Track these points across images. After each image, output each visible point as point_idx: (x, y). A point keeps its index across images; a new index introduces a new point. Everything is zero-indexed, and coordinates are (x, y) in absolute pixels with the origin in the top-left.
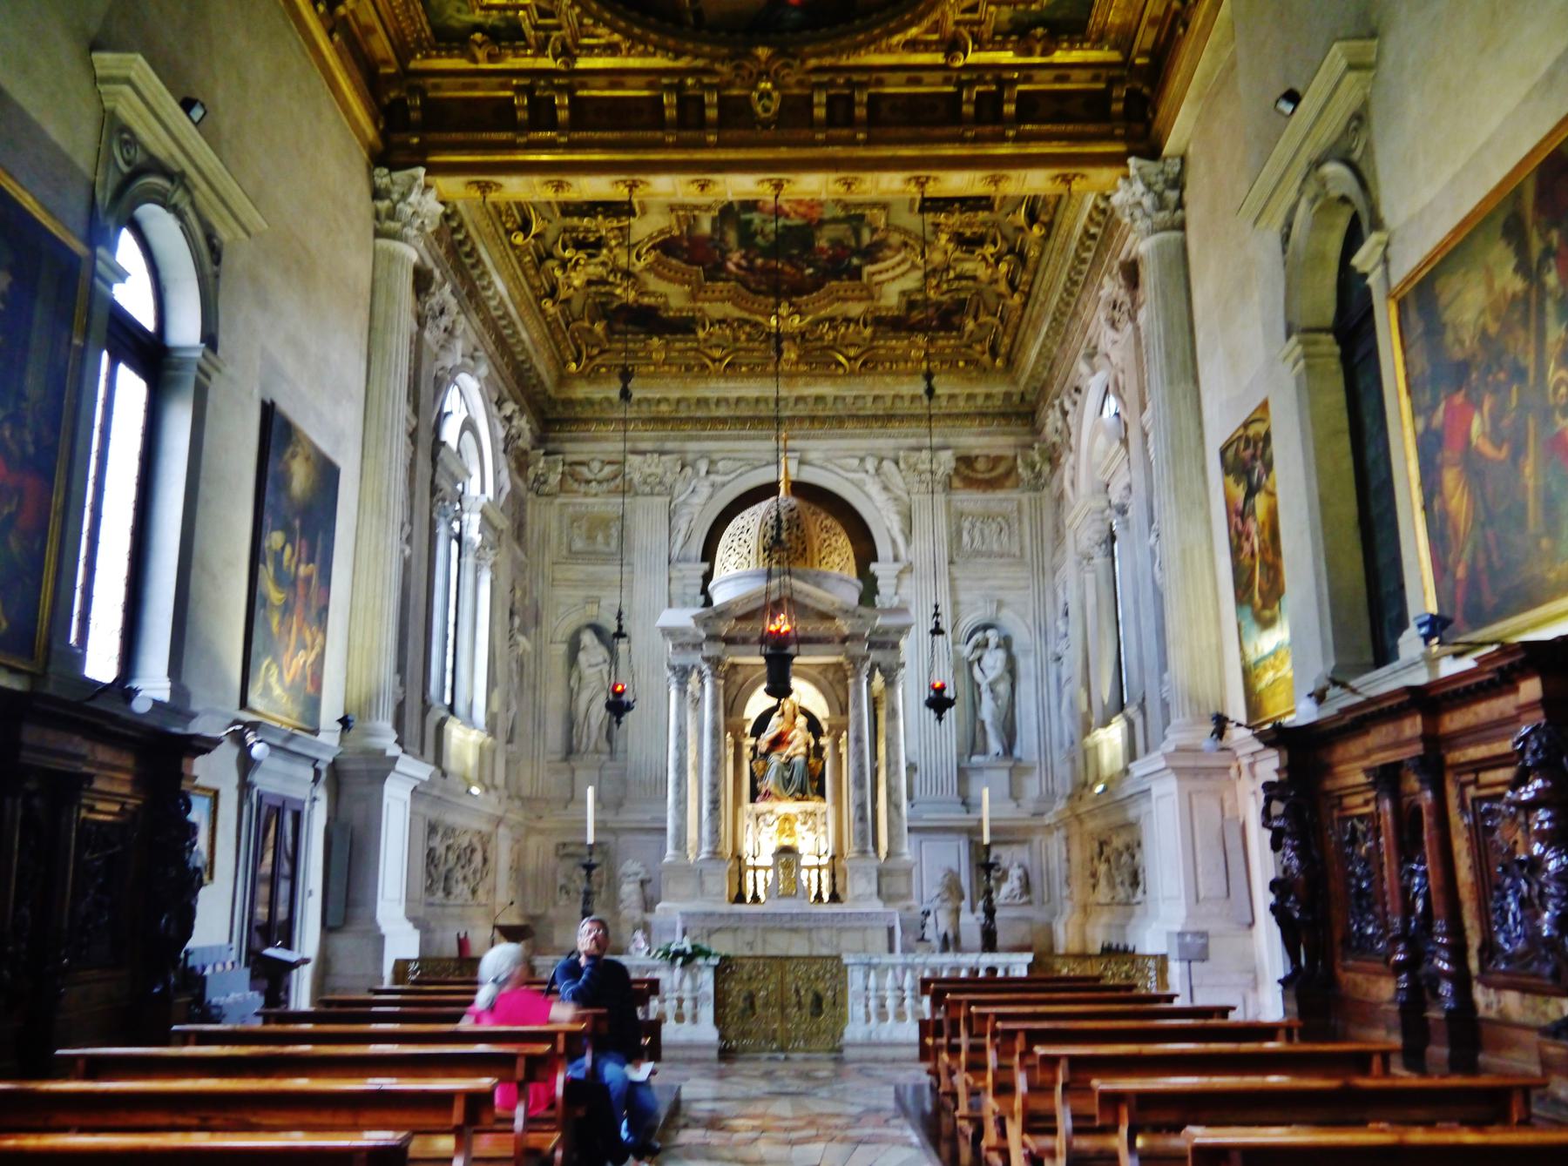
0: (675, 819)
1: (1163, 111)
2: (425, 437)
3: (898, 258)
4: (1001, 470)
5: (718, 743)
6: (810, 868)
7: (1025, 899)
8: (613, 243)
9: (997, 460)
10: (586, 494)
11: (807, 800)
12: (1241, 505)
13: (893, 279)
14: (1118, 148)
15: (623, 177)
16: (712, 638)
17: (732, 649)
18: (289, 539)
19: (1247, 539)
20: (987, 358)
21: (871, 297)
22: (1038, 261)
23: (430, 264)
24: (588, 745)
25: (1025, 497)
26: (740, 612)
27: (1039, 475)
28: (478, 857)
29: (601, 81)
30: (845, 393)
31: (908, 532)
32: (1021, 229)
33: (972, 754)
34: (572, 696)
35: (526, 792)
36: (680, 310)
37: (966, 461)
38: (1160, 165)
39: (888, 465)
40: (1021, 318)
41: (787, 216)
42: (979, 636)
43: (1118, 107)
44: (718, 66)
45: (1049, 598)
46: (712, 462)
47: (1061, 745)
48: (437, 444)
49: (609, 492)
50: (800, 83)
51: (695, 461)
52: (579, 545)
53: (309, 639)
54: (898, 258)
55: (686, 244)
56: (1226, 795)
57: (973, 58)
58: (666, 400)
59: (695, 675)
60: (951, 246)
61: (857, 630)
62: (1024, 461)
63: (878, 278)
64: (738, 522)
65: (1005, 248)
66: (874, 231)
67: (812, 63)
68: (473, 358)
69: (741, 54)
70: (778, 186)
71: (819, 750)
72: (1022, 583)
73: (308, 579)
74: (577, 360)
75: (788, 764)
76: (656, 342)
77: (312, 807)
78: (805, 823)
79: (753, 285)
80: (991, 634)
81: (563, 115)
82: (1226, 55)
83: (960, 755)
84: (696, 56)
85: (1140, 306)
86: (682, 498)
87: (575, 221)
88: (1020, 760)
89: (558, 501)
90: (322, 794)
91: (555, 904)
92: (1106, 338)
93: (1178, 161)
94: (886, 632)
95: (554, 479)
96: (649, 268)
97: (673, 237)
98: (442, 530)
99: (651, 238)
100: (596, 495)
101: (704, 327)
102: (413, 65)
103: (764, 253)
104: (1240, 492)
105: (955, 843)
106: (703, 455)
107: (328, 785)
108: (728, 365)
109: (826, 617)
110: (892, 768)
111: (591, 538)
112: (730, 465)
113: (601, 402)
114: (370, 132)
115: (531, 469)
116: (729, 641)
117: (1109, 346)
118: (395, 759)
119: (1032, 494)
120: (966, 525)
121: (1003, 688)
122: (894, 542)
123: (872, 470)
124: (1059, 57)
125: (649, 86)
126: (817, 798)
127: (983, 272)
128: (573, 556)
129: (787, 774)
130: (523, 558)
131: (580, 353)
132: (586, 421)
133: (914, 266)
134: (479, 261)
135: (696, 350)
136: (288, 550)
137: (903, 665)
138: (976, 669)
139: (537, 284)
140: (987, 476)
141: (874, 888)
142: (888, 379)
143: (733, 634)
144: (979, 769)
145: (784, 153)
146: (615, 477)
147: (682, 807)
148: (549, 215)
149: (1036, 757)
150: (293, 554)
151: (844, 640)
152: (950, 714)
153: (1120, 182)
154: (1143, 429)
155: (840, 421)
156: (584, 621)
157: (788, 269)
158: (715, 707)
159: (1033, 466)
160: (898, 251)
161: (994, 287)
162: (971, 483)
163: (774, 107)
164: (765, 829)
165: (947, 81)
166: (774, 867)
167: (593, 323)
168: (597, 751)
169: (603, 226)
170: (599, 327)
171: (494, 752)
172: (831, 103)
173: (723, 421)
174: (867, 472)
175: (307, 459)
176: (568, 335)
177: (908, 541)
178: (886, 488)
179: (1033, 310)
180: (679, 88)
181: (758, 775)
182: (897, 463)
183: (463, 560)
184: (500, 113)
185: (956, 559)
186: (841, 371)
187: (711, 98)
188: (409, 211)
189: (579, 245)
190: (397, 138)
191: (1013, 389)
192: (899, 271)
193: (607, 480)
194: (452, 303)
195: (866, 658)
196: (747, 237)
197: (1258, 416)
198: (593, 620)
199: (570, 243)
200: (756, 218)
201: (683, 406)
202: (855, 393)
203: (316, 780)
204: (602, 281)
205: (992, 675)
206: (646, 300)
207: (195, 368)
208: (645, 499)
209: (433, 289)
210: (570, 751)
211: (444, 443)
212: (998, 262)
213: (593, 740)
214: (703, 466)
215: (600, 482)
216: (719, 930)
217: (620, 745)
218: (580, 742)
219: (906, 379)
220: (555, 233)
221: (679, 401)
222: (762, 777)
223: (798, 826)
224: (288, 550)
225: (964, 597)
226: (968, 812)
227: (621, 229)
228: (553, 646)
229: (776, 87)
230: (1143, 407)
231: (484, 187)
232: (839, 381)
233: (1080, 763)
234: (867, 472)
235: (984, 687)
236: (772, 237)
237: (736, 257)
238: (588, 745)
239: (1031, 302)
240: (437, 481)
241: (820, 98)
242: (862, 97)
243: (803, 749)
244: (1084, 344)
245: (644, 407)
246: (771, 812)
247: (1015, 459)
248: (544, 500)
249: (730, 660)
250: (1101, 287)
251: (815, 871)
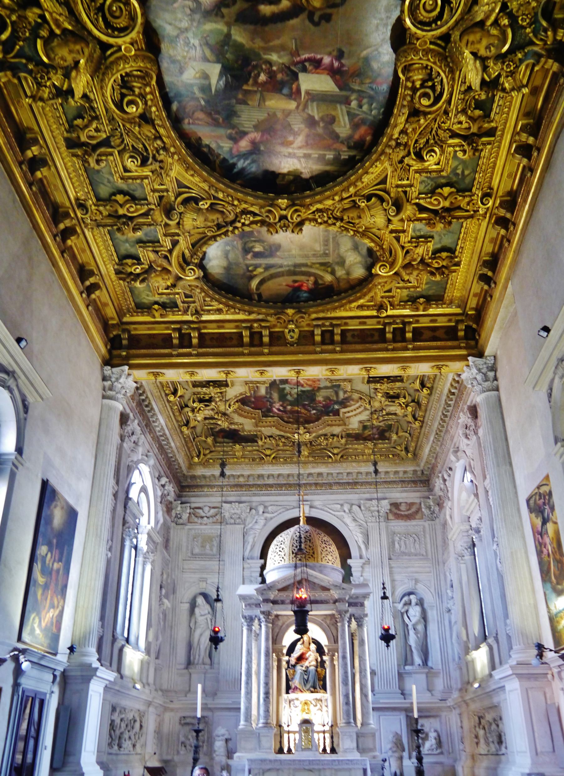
1: (483, 335)
2: (121, 496)
3: (358, 405)
4: (413, 509)
5: (269, 659)
6: (318, 732)
7: (439, 751)
8: (218, 399)
9: (411, 505)
10: (201, 524)
12: (540, 529)
13: (355, 415)
14: (464, 352)
15: (223, 369)
16: (266, 601)
17: (276, 606)
18: (50, 550)
19: (545, 547)
20: (403, 453)
21: (345, 424)
22: (427, 406)
23: (128, 411)
24: (199, 660)
25: (426, 524)
26: (280, 586)
27: (433, 512)
28: (137, 725)
29: (214, 325)
30: (332, 472)
31: (367, 543)
32: (418, 390)
33: (406, 665)
34: (191, 631)
35: (165, 687)
36: (250, 431)
37: (395, 505)
38: (484, 360)
39: (355, 508)
40: (420, 433)
41: (302, 386)
42: (406, 598)
43: (461, 334)
44: (269, 318)
45: (442, 578)
46: (265, 507)
47: (454, 660)
48: (127, 499)
49: (214, 523)
50: (308, 325)
51: (257, 506)
52: (197, 550)
53: (56, 603)
54: (358, 405)
55: (253, 400)
56: (547, 690)
57: (390, 312)
58: (243, 476)
59: (256, 621)
60: (383, 399)
61: (341, 597)
62: (425, 505)
63: (347, 415)
64: (279, 539)
65: (410, 400)
66: (345, 392)
67: (314, 316)
68: (147, 456)
69: (280, 312)
70: (298, 372)
71: (323, 662)
72: (428, 570)
73: (58, 571)
74: (198, 456)
75: (306, 671)
76: (237, 447)
77: (51, 696)
79: (286, 419)
80: (412, 597)
81: (195, 341)
82: (512, 310)
83: (399, 665)
84: (259, 314)
85: (479, 427)
86: (250, 525)
87: (199, 389)
88: (432, 668)
89: (187, 527)
90: (56, 689)
91: (178, 753)
92: (463, 443)
93: (493, 358)
94: (357, 597)
95: (185, 516)
96: (235, 411)
97: (247, 396)
98: (127, 543)
99: (236, 397)
100: (206, 524)
101: (261, 439)
102: (125, 319)
103: (292, 404)
104: (539, 522)
105: (398, 717)
106: (261, 503)
107: (60, 684)
108: (274, 458)
109: (325, 589)
110: (363, 673)
111: (203, 546)
112: (274, 508)
113: (210, 477)
114: (103, 350)
115: (173, 511)
116: (274, 602)
117: (465, 447)
118: (96, 669)
119: (430, 522)
120: (397, 539)
121: (420, 627)
122: (359, 547)
123: (347, 511)
124: (431, 311)
125: (237, 327)
127: (399, 411)
128: (194, 556)
129: (306, 677)
130: (168, 557)
131: (200, 453)
132: (202, 486)
133: (366, 409)
134: (152, 409)
135: (258, 451)
136: (49, 555)
137: (366, 615)
138: (405, 617)
139: (180, 419)
140: (406, 513)
141: (355, 745)
142: (354, 464)
143: (276, 599)
144: (409, 673)
145: (301, 357)
146: (216, 515)
147: (249, 696)
148: (186, 387)
149: (440, 667)
150: (51, 557)
151: (335, 602)
152: (393, 643)
153: (465, 368)
154: (485, 488)
155: (330, 485)
156: (199, 591)
157: (303, 411)
158: (267, 639)
159: (429, 508)
160: (358, 402)
161: (406, 418)
162: (398, 516)
163: (296, 336)
165: (379, 323)
166: (300, 732)
167: (206, 437)
168: (204, 664)
169: (212, 391)
170: (210, 440)
171: (148, 664)
172: (323, 333)
173: (271, 486)
174: (345, 511)
175: (62, 508)
176: (194, 444)
177: (367, 548)
178: (355, 520)
179: (425, 430)
180: (250, 328)
181: (290, 677)
182: (360, 507)
183: (137, 559)
184: (166, 341)
185: (392, 557)
186: (330, 460)
187: (266, 332)
188: (120, 386)
189: (201, 401)
190: (115, 352)
191: (417, 469)
192: (358, 411)
193: (212, 517)
194: (138, 430)
195: (346, 612)
196: (283, 397)
197: (544, 483)
198: (203, 591)
199: (196, 400)
200: (287, 387)
201: (251, 479)
202: (337, 471)
203: (53, 682)
204: (212, 418)
205: (414, 620)
206: (233, 427)
207: (11, 464)
208: (231, 526)
209: (129, 423)
210: (189, 663)
211: (130, 499)
212: (407, 406)
213: (201, 657)
214: (261, 509)
215: (208, 517)
216: (269, 770)
217: (216, 660)
218: (194, 659)
219: (363, 464)
220: (190, 395)
221: (249, 476)
222: (292, 679)
223: (311, 707)
224: (49, 555)
225: (397, 577)
226: (405, 699)
227: (221, 393)
228: (182, 605)
229: (297, 327)
230: (485, 478)
231: (156, 375)
232: (329, 465)
233: (464, 670)
234: (345, 511)
235: (410, 627)
236: (295, 396)
237: (277, 405)
238: (199, 660)
239: (424, 425)
240: (126, 518)
241: (318, 331)
242: (337, 331)
243: (314, 663)
244: (452, 446)
245: (232, 480)
246: (297, 699)
247: (420, 504)
248: (179, 527)
249: (275, 613)
250: (459, 418)
251: (321, 735)
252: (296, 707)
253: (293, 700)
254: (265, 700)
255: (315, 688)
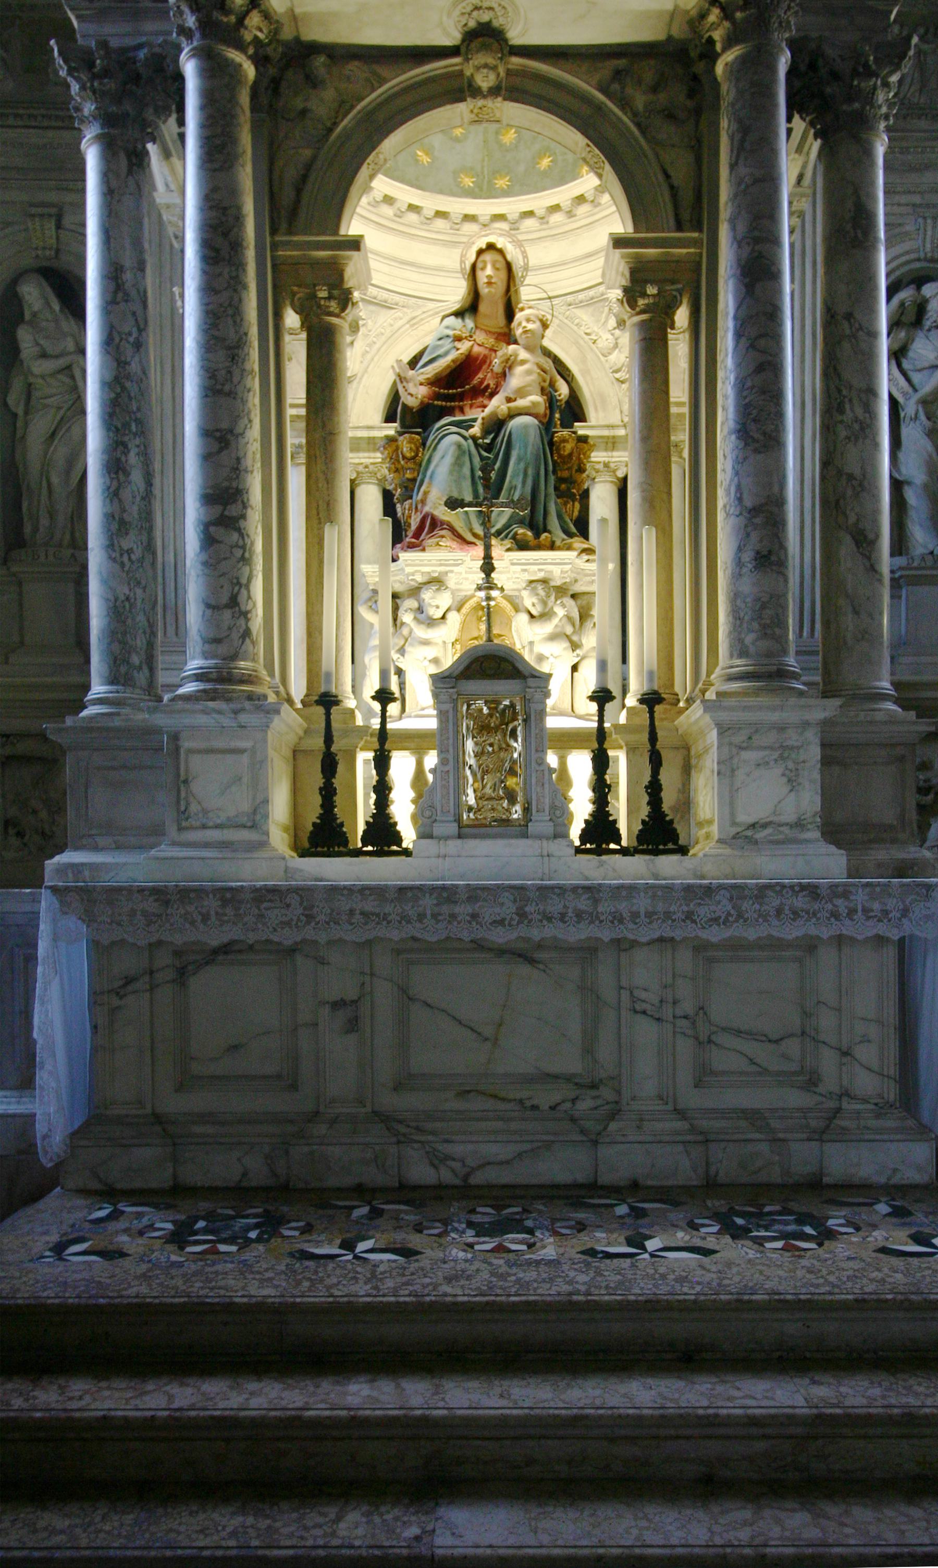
0: (104, 582)
11: (552, 547)
78: (546, 615)
126: (578, 543)
164: (421, 632)
243: (535, 398)
246: (437, 582)
252: (431, 623)
253: (415, 591)
254: (209, 541)
255: (537, 526)
